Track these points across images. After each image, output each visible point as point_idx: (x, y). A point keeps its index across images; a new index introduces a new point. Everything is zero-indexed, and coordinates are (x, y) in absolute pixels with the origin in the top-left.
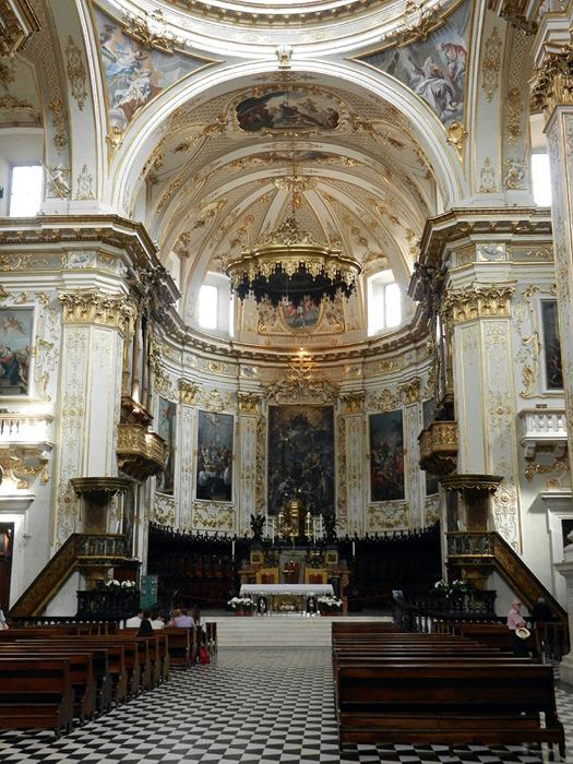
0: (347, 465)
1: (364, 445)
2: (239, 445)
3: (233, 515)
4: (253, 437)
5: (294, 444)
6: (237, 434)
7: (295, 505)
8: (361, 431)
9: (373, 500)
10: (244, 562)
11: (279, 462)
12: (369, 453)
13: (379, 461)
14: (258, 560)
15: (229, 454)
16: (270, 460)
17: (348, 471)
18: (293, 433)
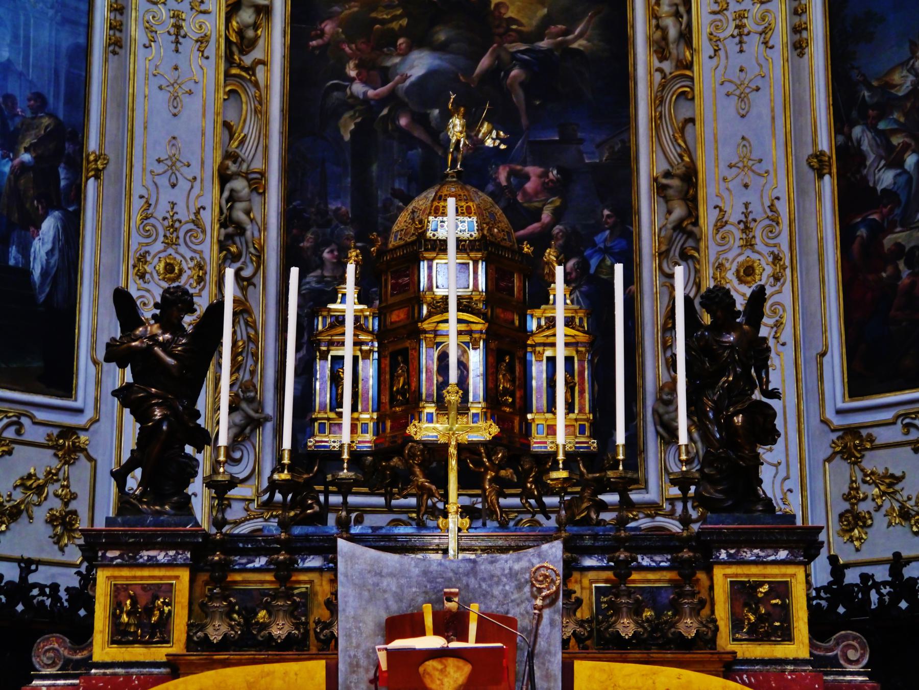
0: (707, 218)
1: (796, 104)
2: (121, 103)
3: (79, 474)
4: (207, 73)
5: (421, 119)
6: (116, 45)
7: (452, 224)
8: (781, 35)
9: (859, 383)
10: (49, 649)
11: (340, 205)
12: (824, 144)
13: (887, 178)
14: (159, 632)
15: (78, 134)
16: (289, 195)
17: (710, 250)
18: (419, 65)
